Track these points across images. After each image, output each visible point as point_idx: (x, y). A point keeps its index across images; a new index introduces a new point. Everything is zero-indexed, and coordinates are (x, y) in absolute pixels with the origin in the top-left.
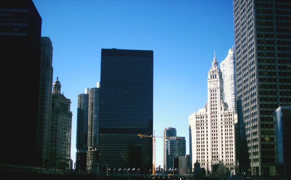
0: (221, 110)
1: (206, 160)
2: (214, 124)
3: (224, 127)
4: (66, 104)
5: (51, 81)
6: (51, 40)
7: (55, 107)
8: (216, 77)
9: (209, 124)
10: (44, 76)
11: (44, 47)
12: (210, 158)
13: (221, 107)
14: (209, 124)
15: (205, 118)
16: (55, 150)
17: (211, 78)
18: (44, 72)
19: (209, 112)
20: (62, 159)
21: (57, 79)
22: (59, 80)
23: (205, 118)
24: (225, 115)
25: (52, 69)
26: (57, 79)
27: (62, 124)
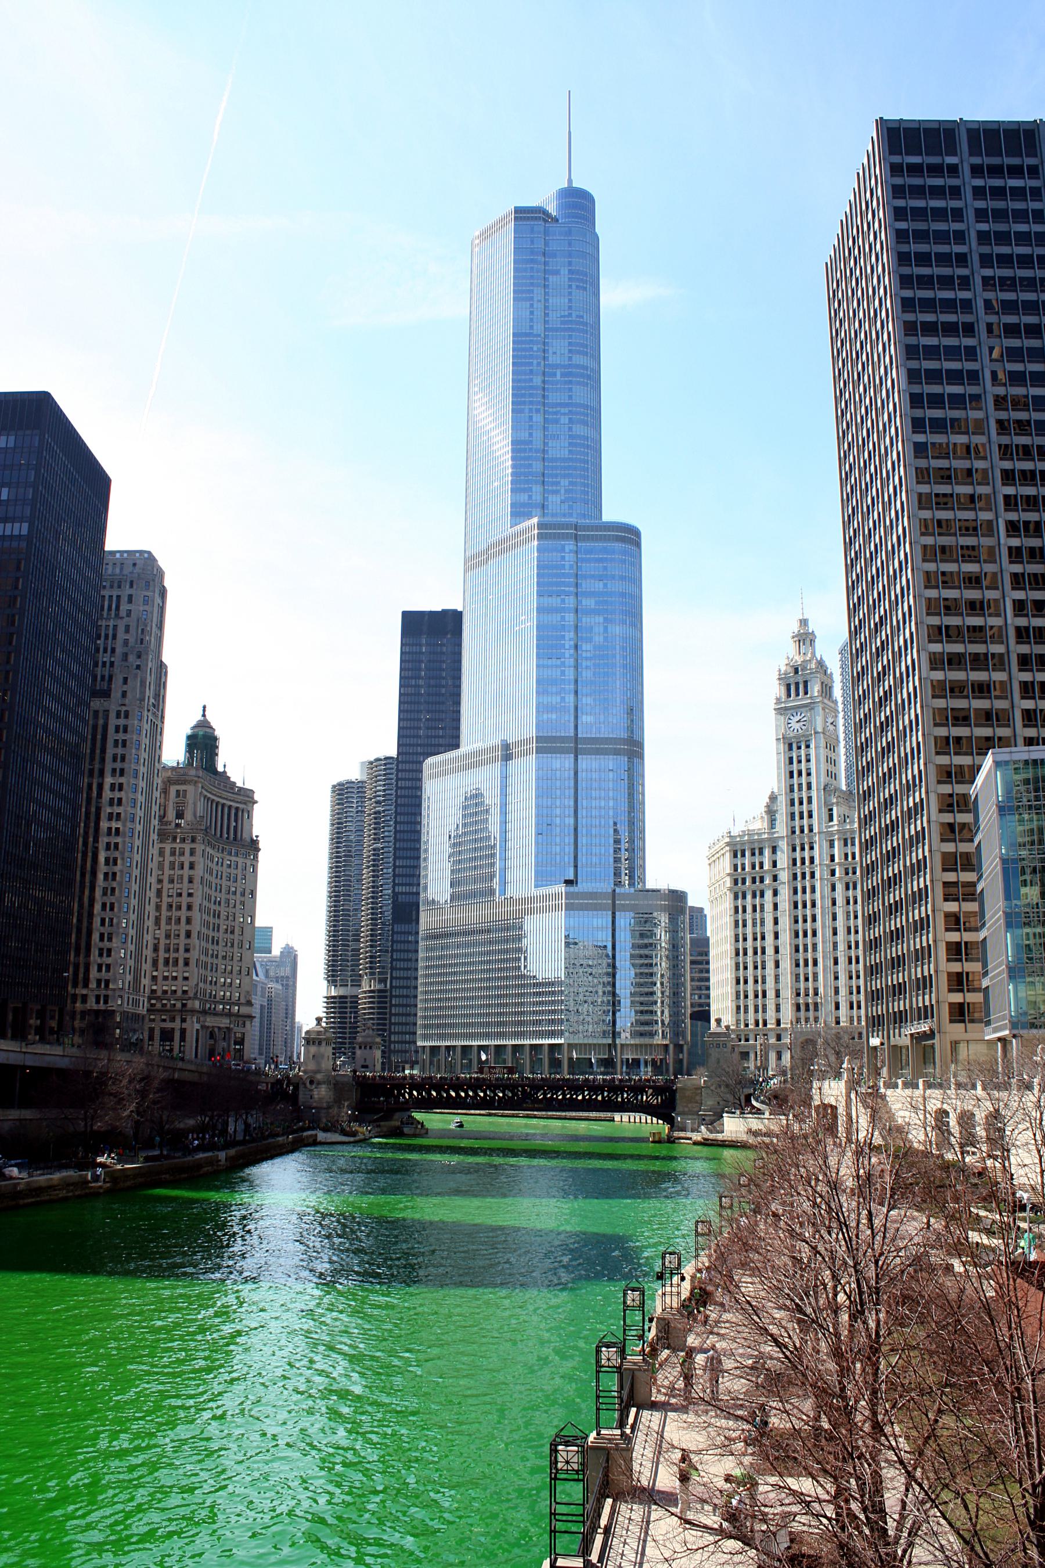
0: (831, 819)
1: (774, 1021)
2: (804, 875)
3: (840, 887)
4: (237, 809)
5: (156, 716)
6: (162, 563)
7: (189, 815)
8: (806, 693)
9: (784, 876)
10: (124, 694)
11: (131, 586)
12: (787, 1014)
13: (831, 810)
14: (784, 876)
15: (767, 852)
16: (186, 979)
17: (789, 695)
18: (125, 680)
19: (782, 828)
20: (216, 1014)
21: (204, 715)
22: (209, 717)
23: (767, 852)
24: (845, 840)
25: (161, 669)
26: (204, 715)
27: (219, 881)
